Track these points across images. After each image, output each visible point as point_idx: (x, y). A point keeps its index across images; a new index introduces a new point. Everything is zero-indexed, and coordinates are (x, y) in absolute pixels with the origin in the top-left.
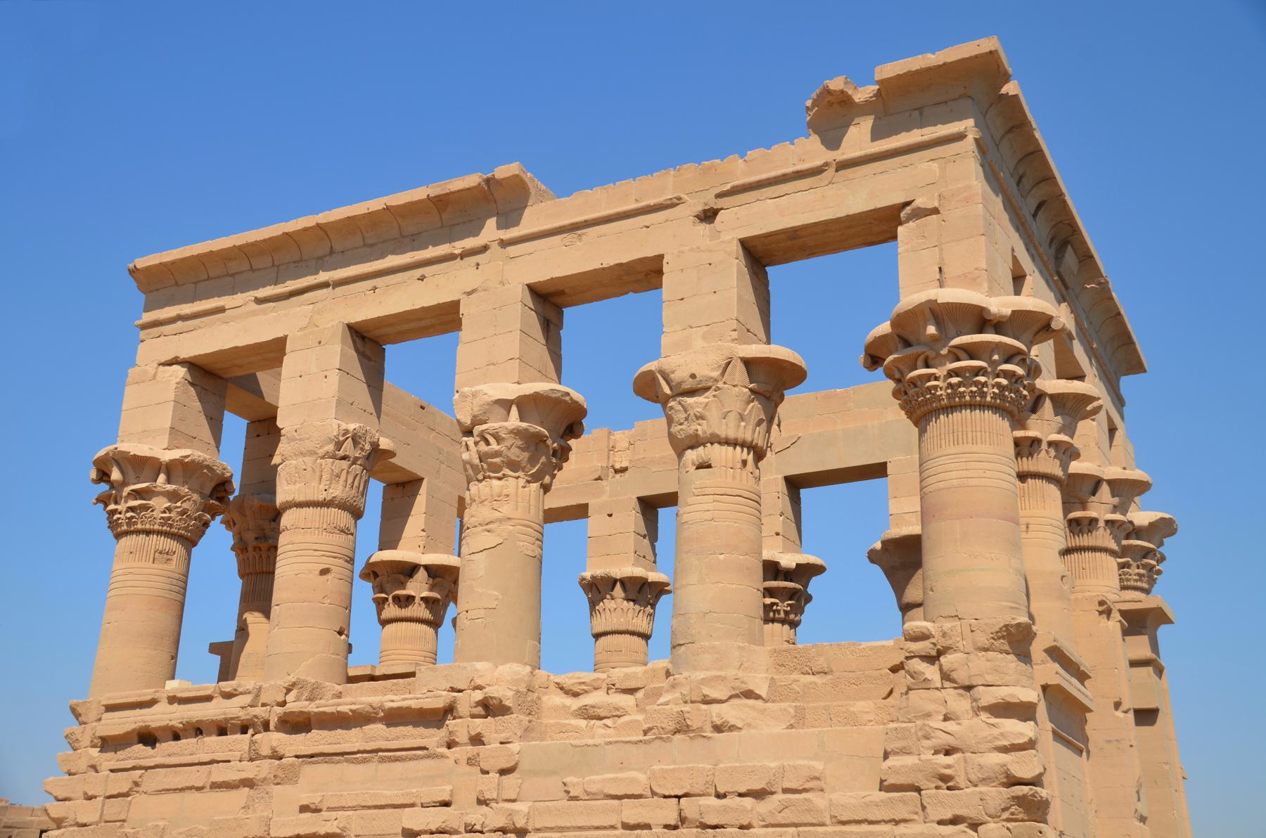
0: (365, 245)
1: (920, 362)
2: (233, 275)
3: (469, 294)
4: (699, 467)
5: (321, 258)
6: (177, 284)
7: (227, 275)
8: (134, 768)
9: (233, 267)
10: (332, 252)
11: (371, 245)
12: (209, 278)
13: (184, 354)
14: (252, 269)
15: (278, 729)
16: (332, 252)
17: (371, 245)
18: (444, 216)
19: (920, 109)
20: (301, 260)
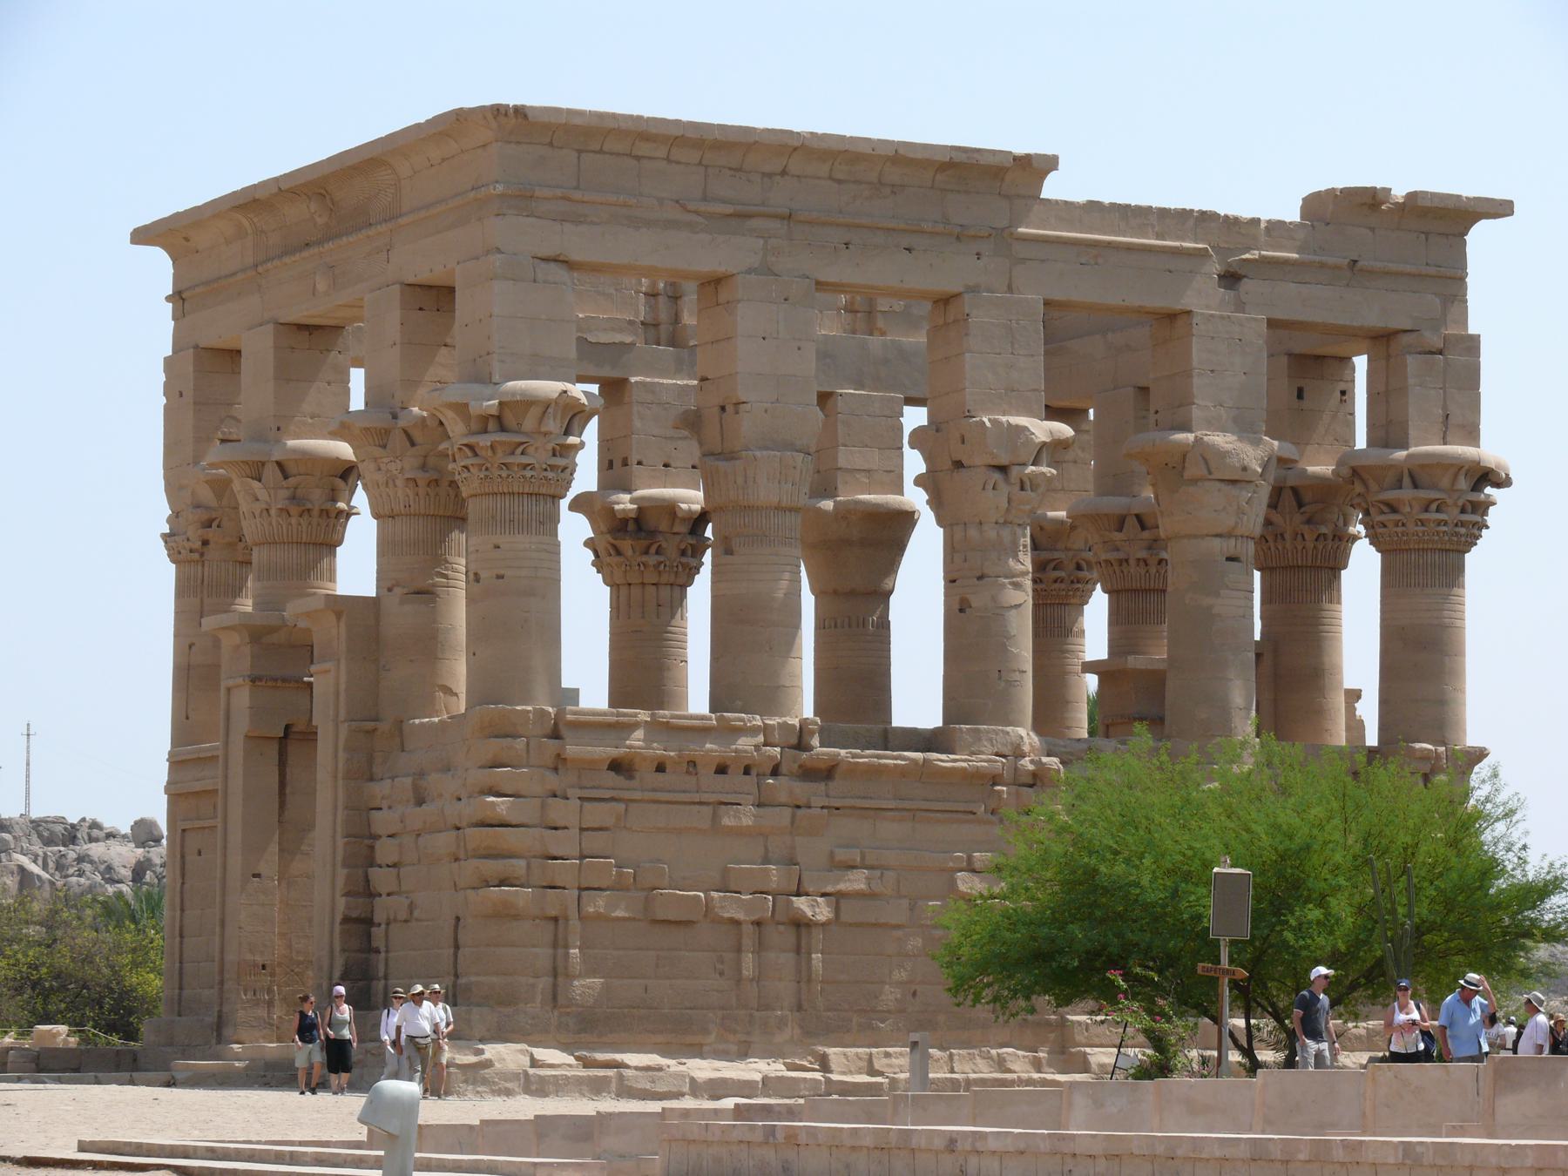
0: (830, 178)
1: (1434, 506)
2: (638, 158)
3: (974, 289)
4: (1228, 559)
5: (770, 175)
6: (551, 144)
7: (630, 155)
8: (613, 799)
9: (644, 149)
10: (784, 173)
11: (839, 182)
12: (601, 152)
13: (575, 256)
14: (668, 160)
15: (791, 775)
16: (784, 173)
17: (839, 182)
18: (939, 177)
19: (1427, 234)
20: (738, 170)
